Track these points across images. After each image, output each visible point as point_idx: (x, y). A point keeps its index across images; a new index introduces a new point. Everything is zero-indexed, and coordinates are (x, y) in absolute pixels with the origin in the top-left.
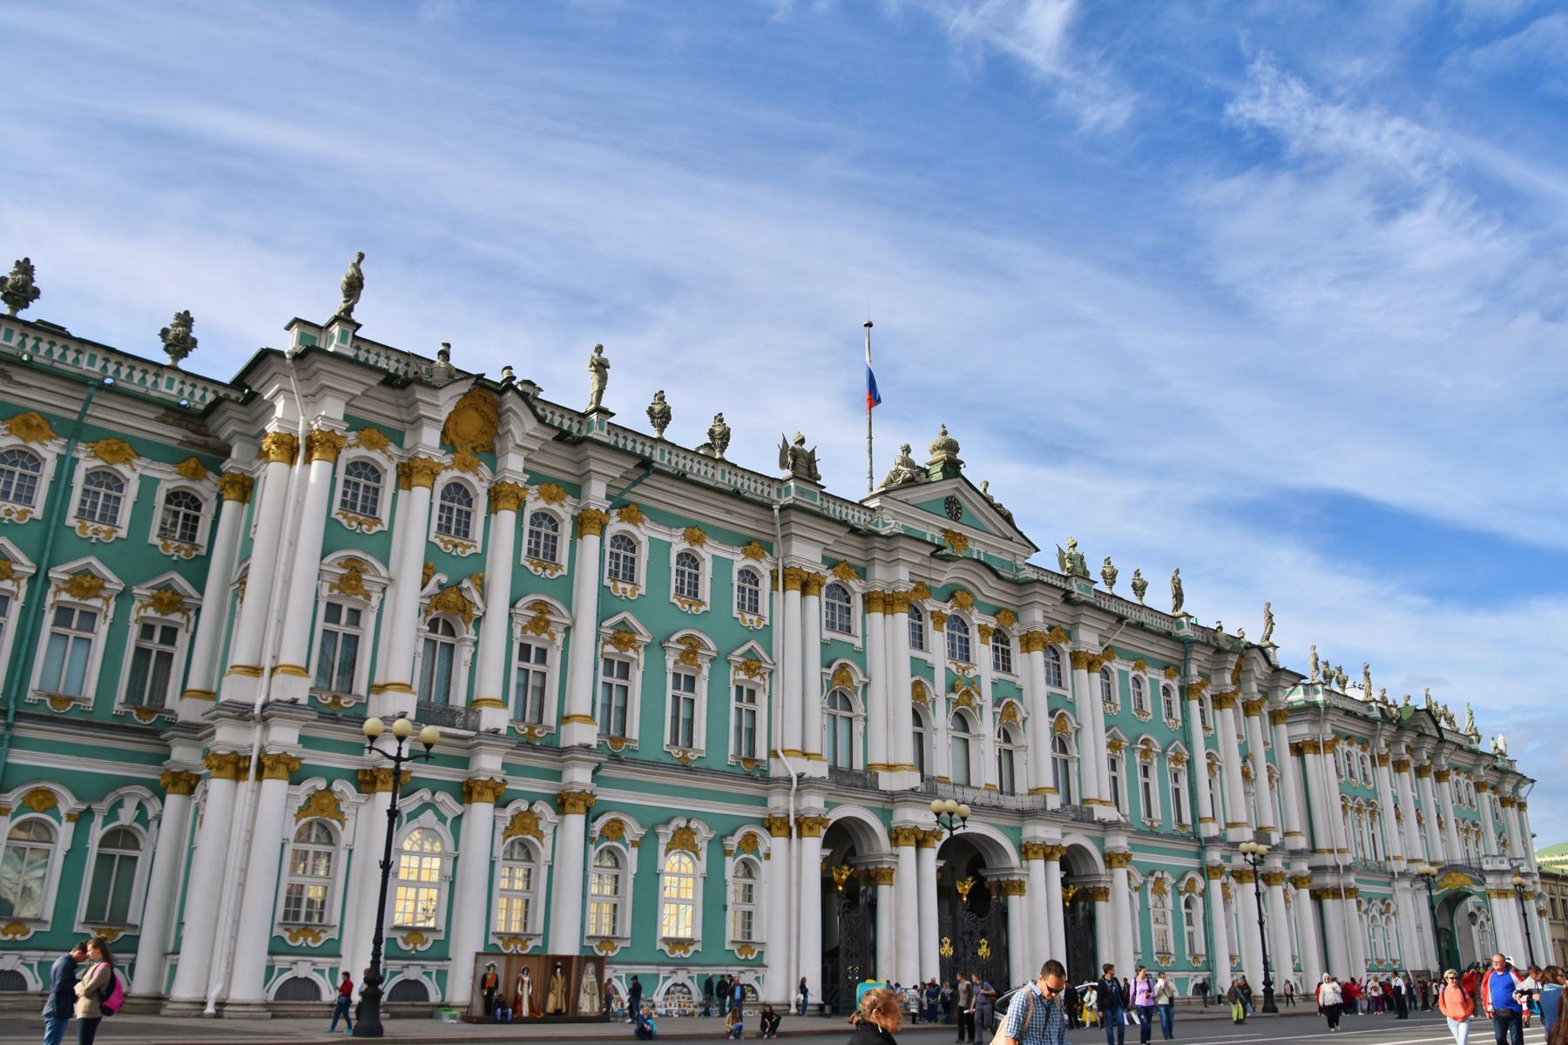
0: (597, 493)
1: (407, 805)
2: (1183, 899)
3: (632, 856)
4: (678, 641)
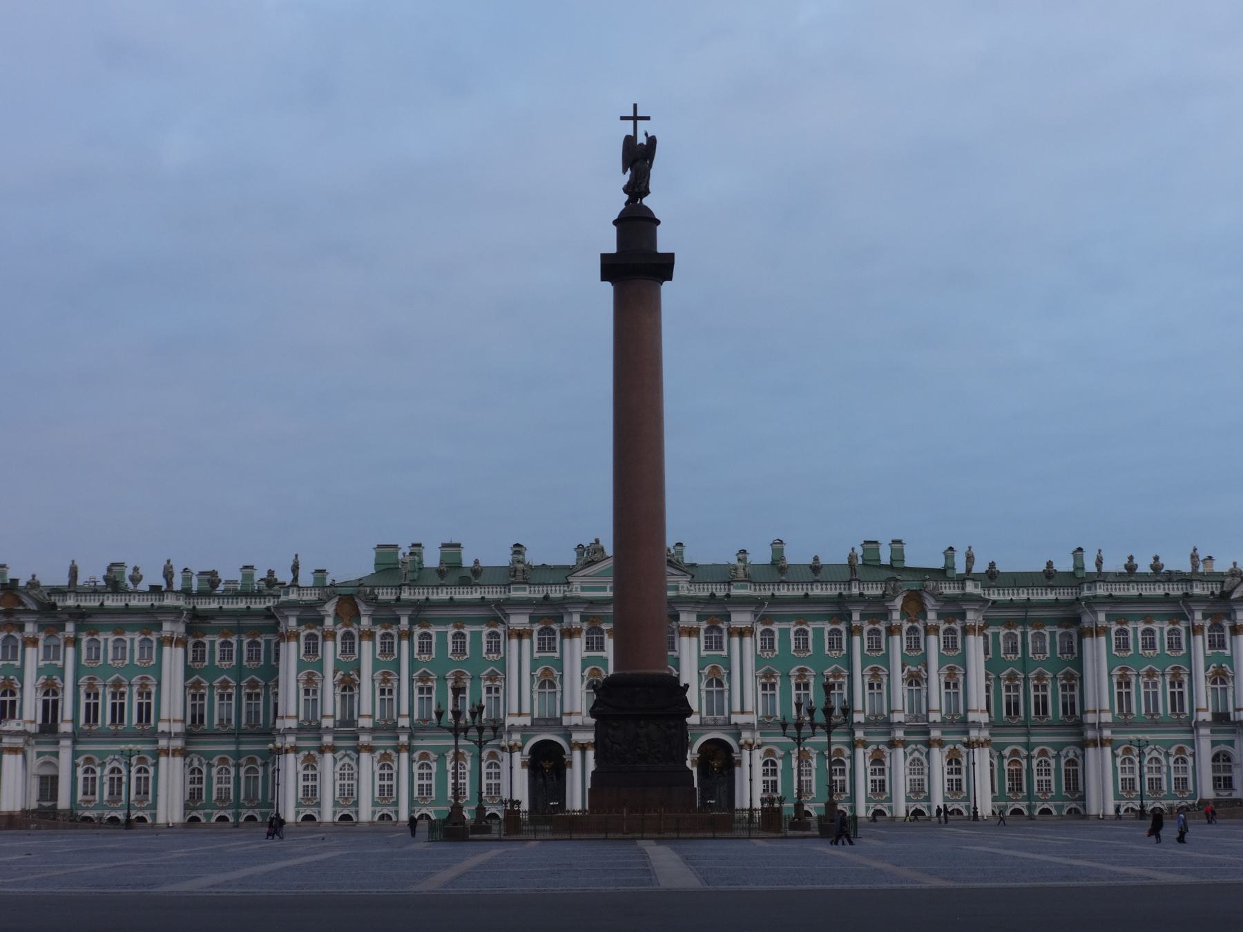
0: (404, 621)
1: (339, 755)
3: (434, 765)
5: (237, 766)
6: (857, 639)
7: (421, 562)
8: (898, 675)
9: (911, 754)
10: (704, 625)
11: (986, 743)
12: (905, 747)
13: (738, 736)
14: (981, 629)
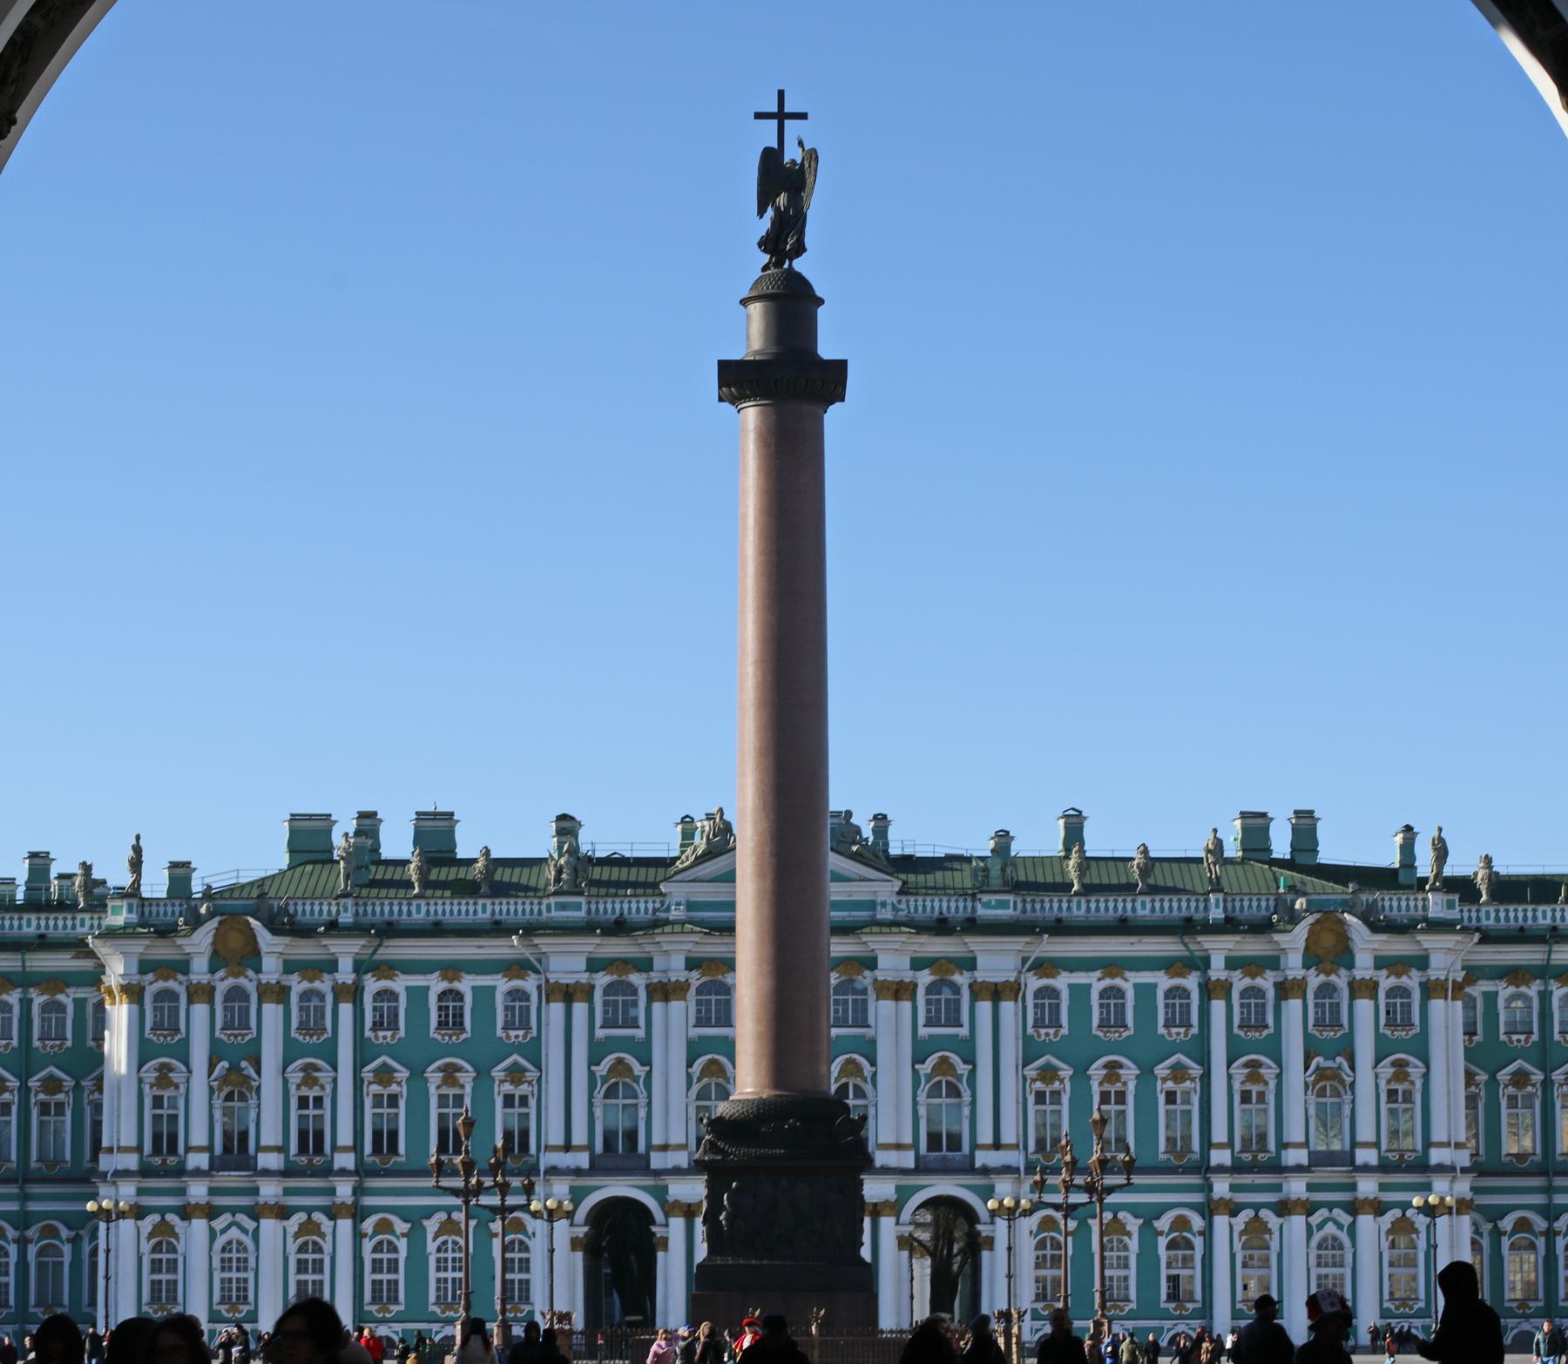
1: (219, 1223)
2: (1162, 1242)
3: (402, 1245)
4: (439, 1069)
5: (22, 1243)
6: (1218, 1006)
7: (376, 849)
8: (1296, 1076)
9: (1321, 1226)
10: (925, 978)
11: (1463, 1206)
12: (1309, 1213)
13: (987, 1193)
14: (1458, 988)
